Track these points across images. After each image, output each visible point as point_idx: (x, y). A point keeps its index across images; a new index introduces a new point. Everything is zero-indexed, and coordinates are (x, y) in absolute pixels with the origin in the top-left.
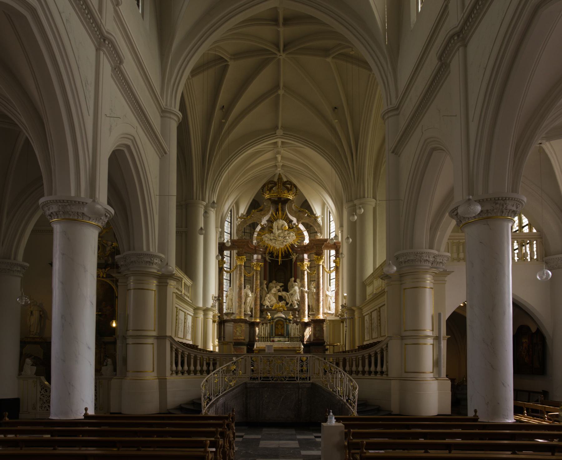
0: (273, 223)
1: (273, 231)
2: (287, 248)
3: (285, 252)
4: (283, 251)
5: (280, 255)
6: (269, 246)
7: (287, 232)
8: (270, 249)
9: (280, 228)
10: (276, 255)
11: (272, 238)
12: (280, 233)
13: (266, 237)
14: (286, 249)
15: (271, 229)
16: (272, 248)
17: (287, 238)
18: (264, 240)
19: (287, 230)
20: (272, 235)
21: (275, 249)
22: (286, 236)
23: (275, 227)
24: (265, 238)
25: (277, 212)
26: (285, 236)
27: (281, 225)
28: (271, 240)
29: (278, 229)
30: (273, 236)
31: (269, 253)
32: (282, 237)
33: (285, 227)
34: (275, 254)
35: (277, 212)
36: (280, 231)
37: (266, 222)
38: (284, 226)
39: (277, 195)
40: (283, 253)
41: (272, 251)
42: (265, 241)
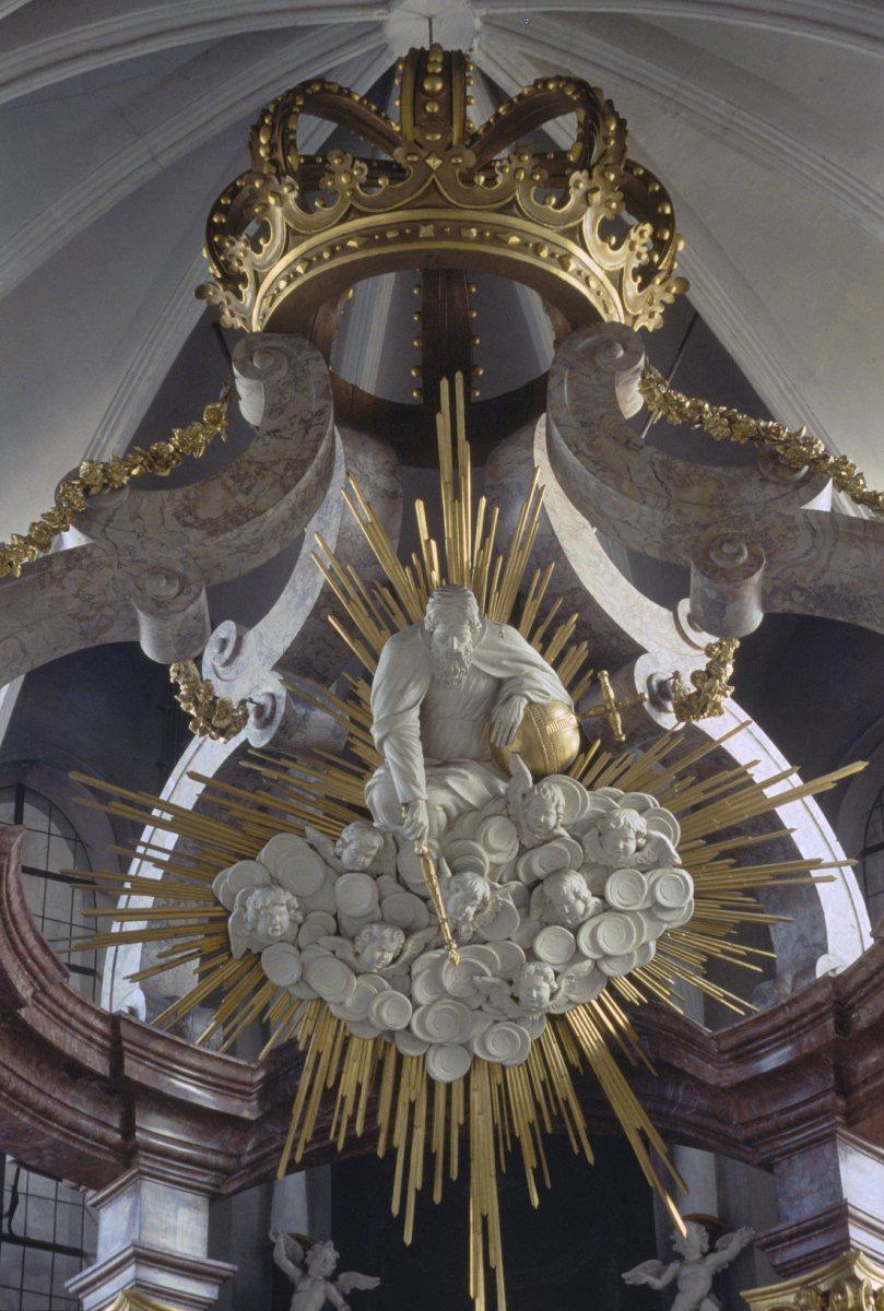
0: (369, 679)
1: (374, 797)
2: (583, 1076)
3: (554, 1143)
4: (523, 1116)
5: (485, 1199)
6: (325, 1042)
7: (571, 797)
8: (330, 1094)
9: (457, 735)
10: (424, 1195)
11: (358, 895)
12: (465, 810)
13: (274, 882)
14: (564, 1086)
15: (339, 784)
16: (356, 1072)
17: (576, 883)
18: (238, 948)
19: (567, 770)
20: (354, 842)
21: (412, 1090)
22: (558, 873)
23: (393, 717)
24: (256, 899)
25: (420, 507)
26: (538, 864)
27: (483, 685)
28: (338, 933)
29: (439, 763)
30: (376, 877)
31: (318, 1155)
32: (497, 876)
33: (537, 713)
34: (416, 1180)
35: (420, 507)
36: (469, 785)
37: (273, 685)
38: (519, 709)
39: (407, 232)
40: (530, 1160)
41: (371, 1134)
42: (253, 959)
